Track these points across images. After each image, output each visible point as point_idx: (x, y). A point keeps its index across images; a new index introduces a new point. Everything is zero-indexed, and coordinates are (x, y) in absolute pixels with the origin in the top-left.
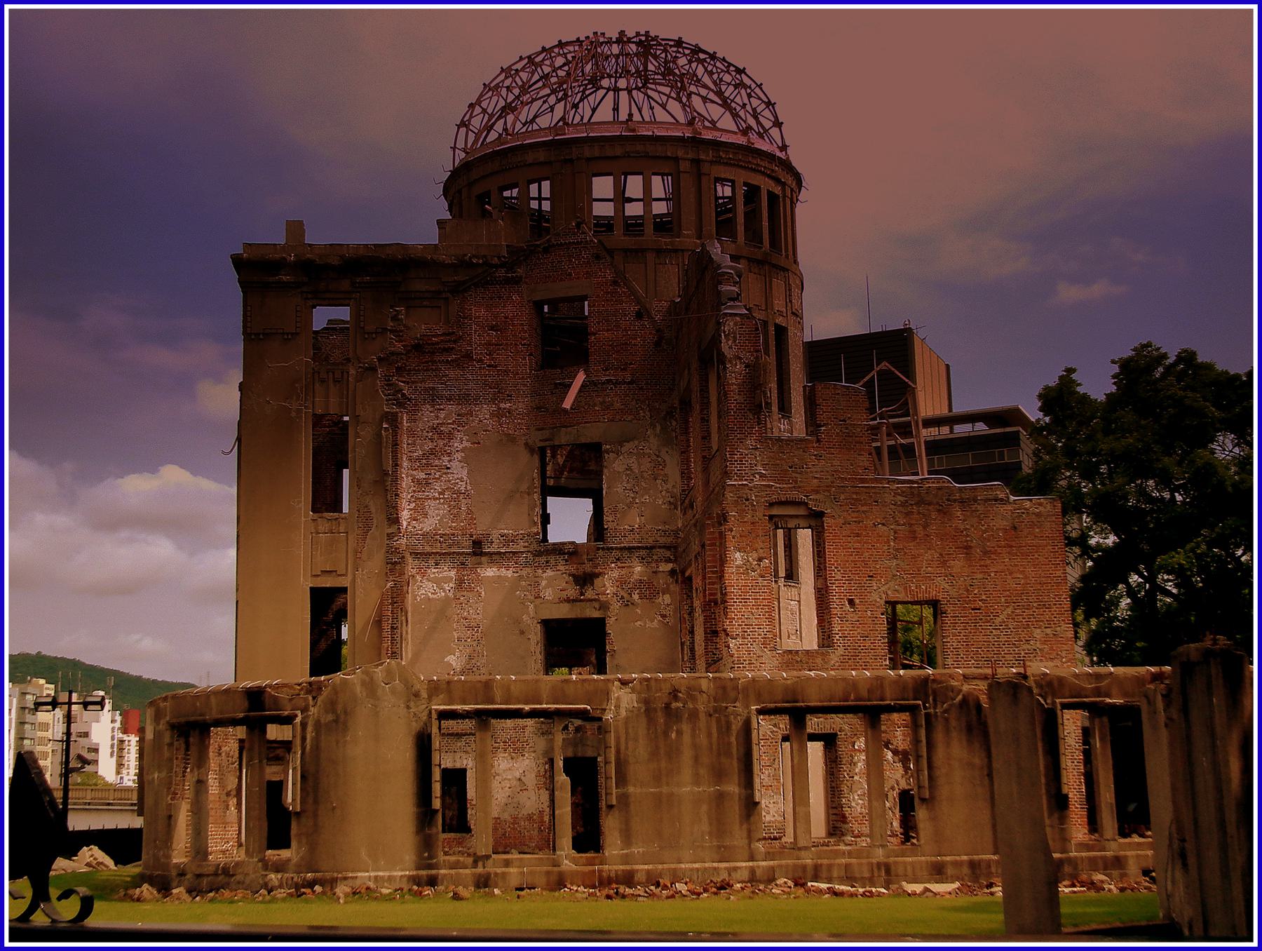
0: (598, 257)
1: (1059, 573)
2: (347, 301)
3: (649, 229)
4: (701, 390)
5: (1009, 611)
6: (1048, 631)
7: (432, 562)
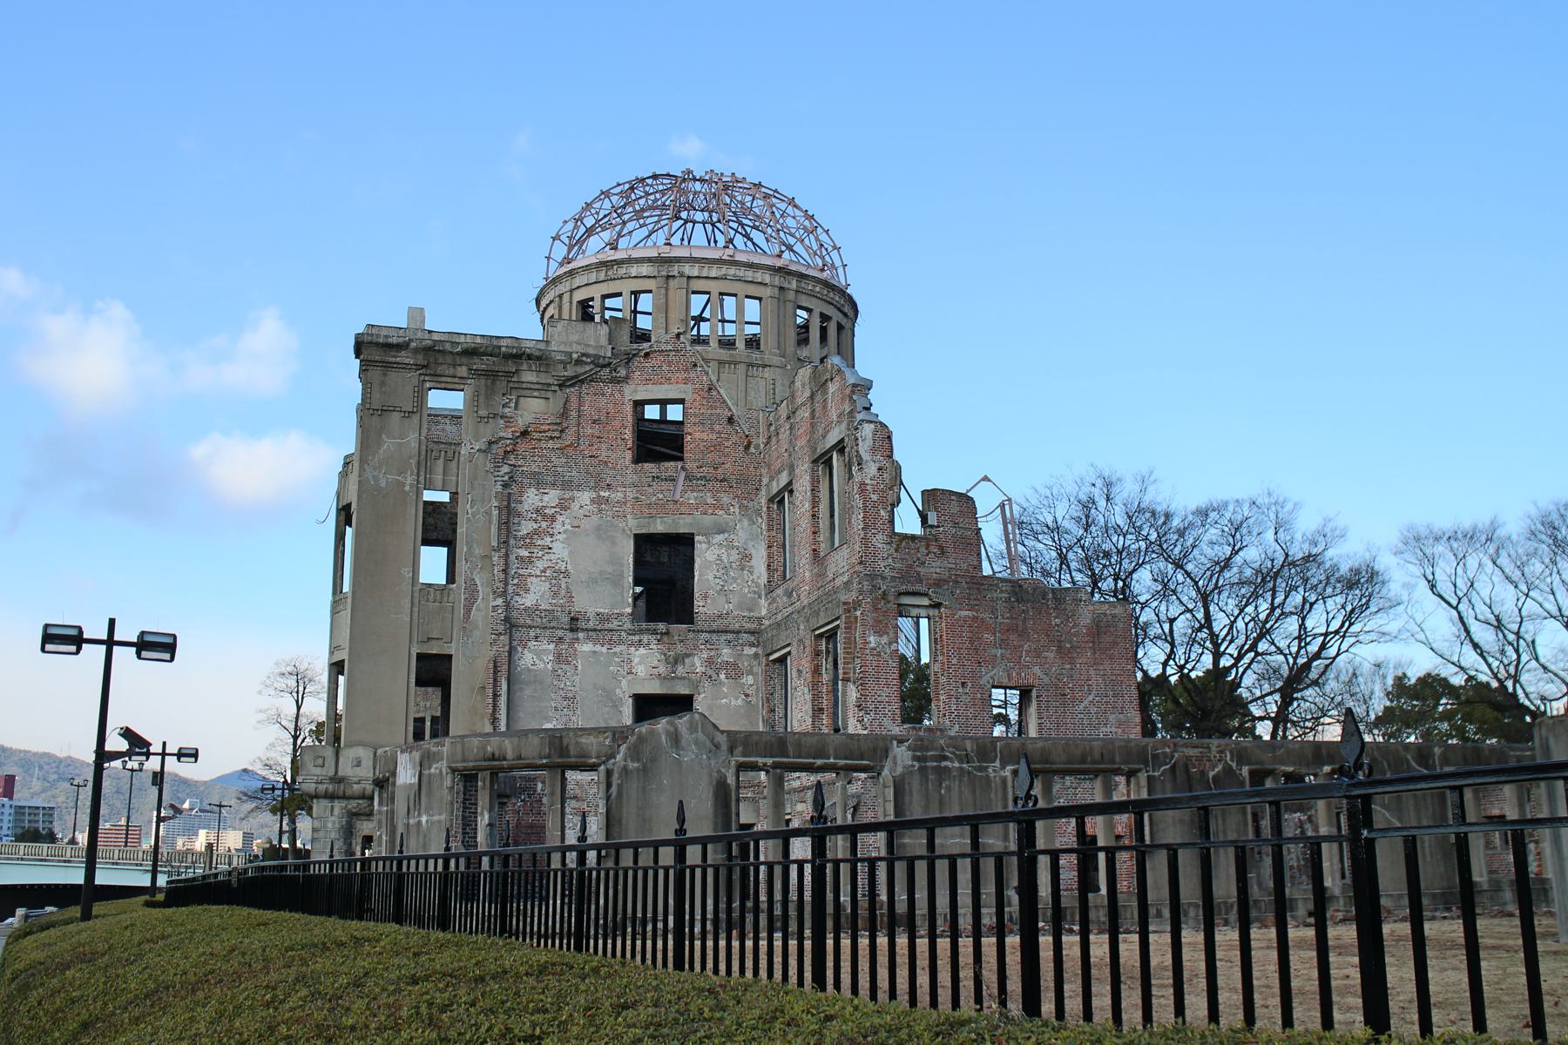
0: (695, 365)
1: (1129, 667)
2: (462, 387)
3: (740, 345)
4: (813, 490)
5: (1091, 698)
6: (1121, 716)
7: (532, 634)
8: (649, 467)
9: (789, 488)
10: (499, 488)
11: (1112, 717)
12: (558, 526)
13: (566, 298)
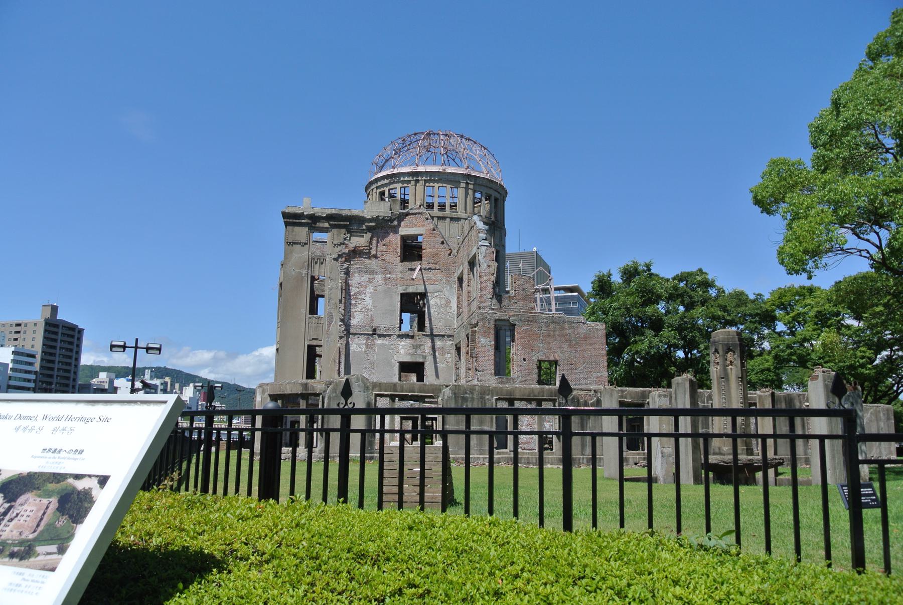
0: (427, 219)
3: (448, 208)
5: (584, 365)
8: (408, 264)
9: (462, 273)
10: (342, 275)
11: (594, 375)
12: (368, 290)
13: (375, 190)
